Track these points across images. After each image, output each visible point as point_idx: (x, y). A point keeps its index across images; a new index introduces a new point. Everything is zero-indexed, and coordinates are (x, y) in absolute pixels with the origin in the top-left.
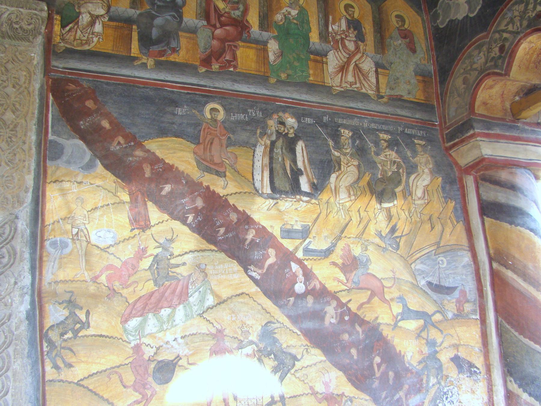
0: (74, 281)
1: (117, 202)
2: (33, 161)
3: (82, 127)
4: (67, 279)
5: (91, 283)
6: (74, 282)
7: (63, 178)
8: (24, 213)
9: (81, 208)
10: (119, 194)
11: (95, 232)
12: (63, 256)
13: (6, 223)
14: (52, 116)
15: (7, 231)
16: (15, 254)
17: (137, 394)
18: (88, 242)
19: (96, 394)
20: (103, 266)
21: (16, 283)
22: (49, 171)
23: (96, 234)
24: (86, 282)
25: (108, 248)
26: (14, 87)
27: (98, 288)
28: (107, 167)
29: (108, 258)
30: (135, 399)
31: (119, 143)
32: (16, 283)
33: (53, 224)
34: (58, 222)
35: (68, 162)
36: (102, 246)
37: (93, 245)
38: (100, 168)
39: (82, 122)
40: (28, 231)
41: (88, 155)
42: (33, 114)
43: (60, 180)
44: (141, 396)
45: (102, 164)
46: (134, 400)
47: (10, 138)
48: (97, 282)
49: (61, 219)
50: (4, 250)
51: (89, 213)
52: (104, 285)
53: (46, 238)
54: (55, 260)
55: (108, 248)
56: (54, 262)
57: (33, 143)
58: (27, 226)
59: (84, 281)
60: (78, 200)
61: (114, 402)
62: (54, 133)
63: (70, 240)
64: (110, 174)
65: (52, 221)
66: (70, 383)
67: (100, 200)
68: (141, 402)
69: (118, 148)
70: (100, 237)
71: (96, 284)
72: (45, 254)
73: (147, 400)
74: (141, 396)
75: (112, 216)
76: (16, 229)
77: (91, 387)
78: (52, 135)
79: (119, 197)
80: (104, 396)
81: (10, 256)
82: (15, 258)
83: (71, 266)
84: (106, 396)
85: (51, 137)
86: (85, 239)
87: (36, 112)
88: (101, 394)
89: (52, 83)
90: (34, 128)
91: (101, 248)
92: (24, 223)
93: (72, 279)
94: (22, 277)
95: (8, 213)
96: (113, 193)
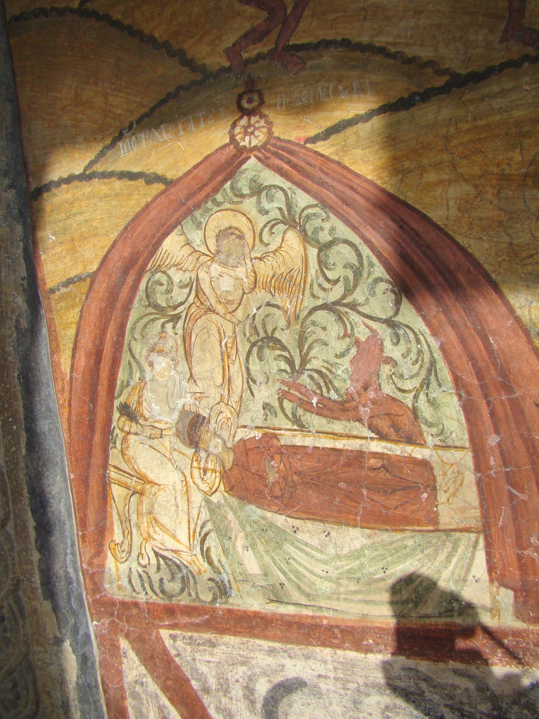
17: (250, 10)
19: (133, 32)
30: (247, 26)
44: (264, 14)
46: (242, 32)
61: (186, 46)
66: (61, 12)
68: (267, 33)
73: (284, 23)
74: (264, 14)
77: (117, 16)
80: (157, 35)
84: (160, 33)
88: (146, 31)
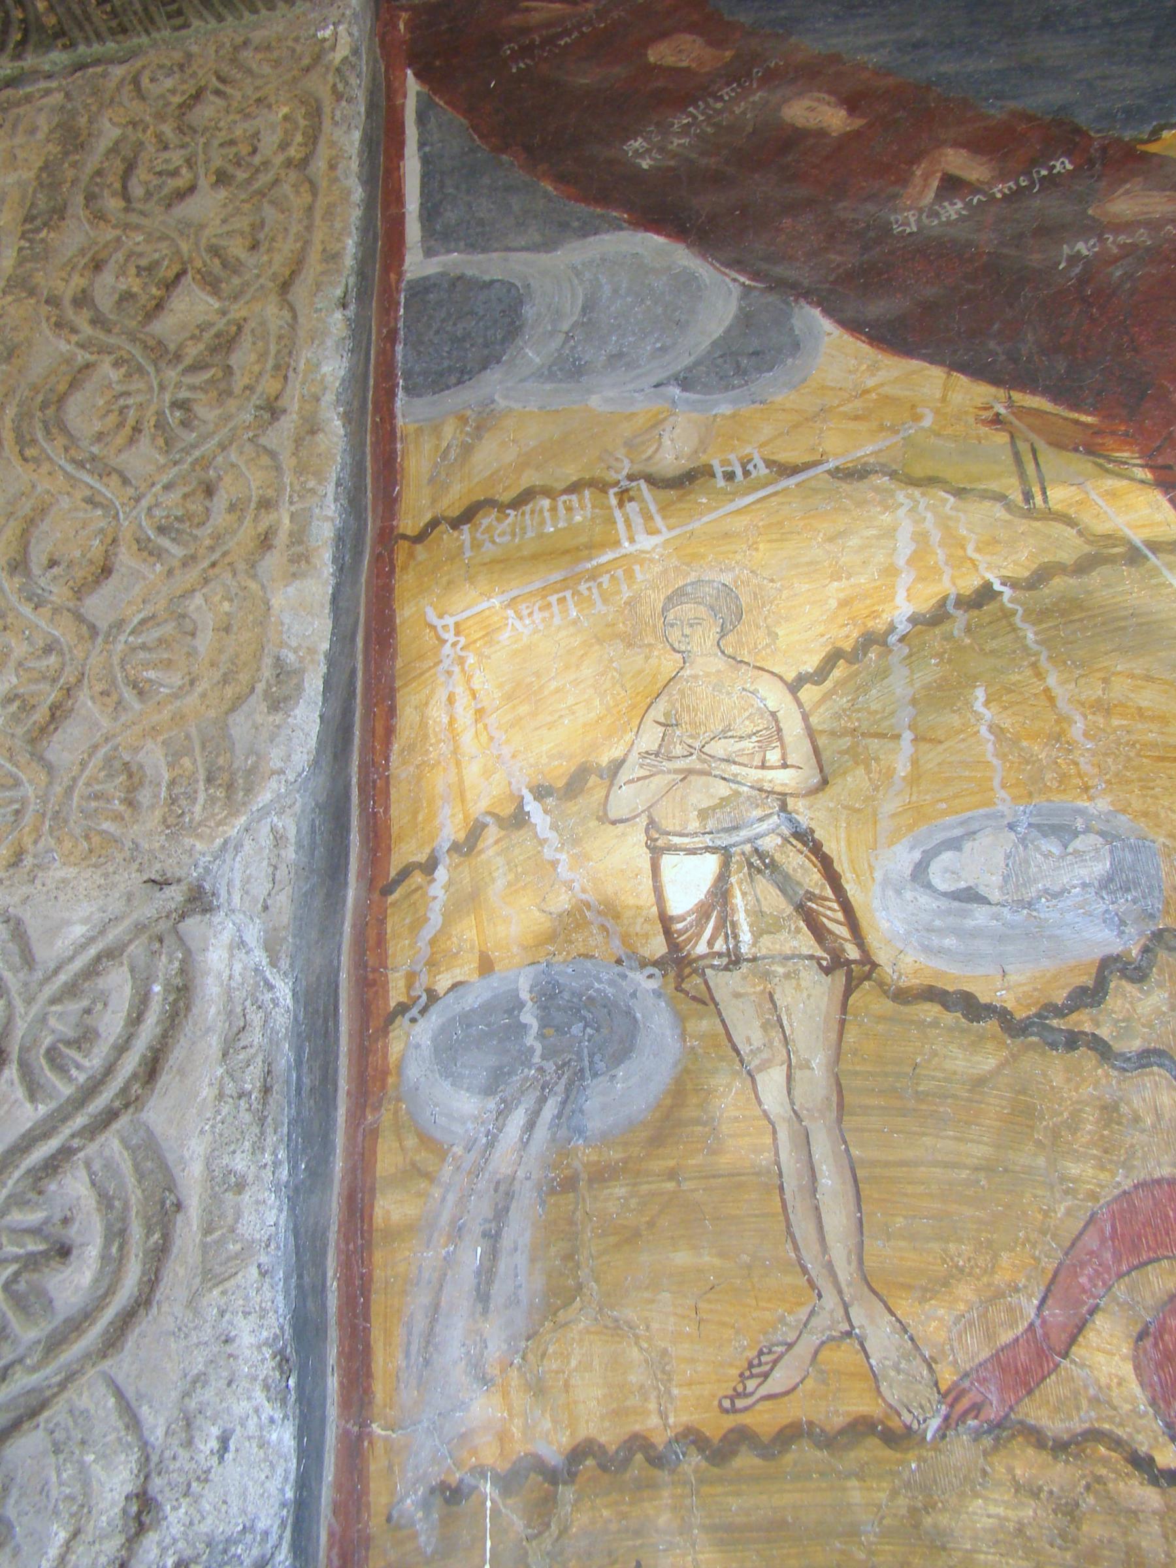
0: (741, 1437)
1: (1066, 556)
2: (331, 489)
3: (645, 164)
4: (656, 1425)
5: (962, 1450)
6: (745, 1460)
7: (530, 478)
8: (255, 855)
9: (718, 663)
10: (1059, 496)
11: (903, 858)
12: (585, 1155)
13: (111, 954)
14: (426, 160)
15: (112, 1024)
16: (165, 1211)
18: (852, 970)
20: (1066, 1215)
21: (143, 1511)
22: (417, 463)
23: (919, 873)
24: (897, 1438)
25: (1091, 995)
26: (222, 178)
27: (1070, 1511)
28: (893, 337)
29: (1110, 1112)
31: (952, 185)
32: (143, 1511)
33: (468, 846)
34: (518, 819)
35: (570, 370)
36: (1011, 984)
37: (903, 996)
38: (835, 356)
39: (638, 144)
40: (284, 991)
41: (719, 296)
42: (331, 257)
43: (506, 497)
45: (854, 326)
47: (182, 405)
48: (1036, 1437)
49: (541, 792)
50: (75, 1187)
51: (809, 693)
52: (1142, 1464)
53: (396, 994)
54: (501, 1214)
55: (1091, 995)
56: (493, 1238)
57: (329, 397)
58: (271, 949)
59: (861, 1428)
60: (687, 610)
62: (438, 235)
63: (645, 982)
64: (936, 373)
65: (451, 828)
67: (890, 572)
69: (953, 209)
70: (970, 896)
71: (1025, 1462)
72: (387, 1160)
75: (1052, 680)
76: (183, 993)
78: (429, 253)
79: (1070, 522)
81: (117, 1234)
82: (160, 1254)
83: (682, 1258)
85: (417, 264)
86: (806, 943)
87: (350, 244)
89: (411, 27)
90: (337, 322)
91: (1003, 1015)
92: (253, 934)
93: (715, 1426)
94: (208, 1444)
95: (130, 879)
96: (1001, 498)
